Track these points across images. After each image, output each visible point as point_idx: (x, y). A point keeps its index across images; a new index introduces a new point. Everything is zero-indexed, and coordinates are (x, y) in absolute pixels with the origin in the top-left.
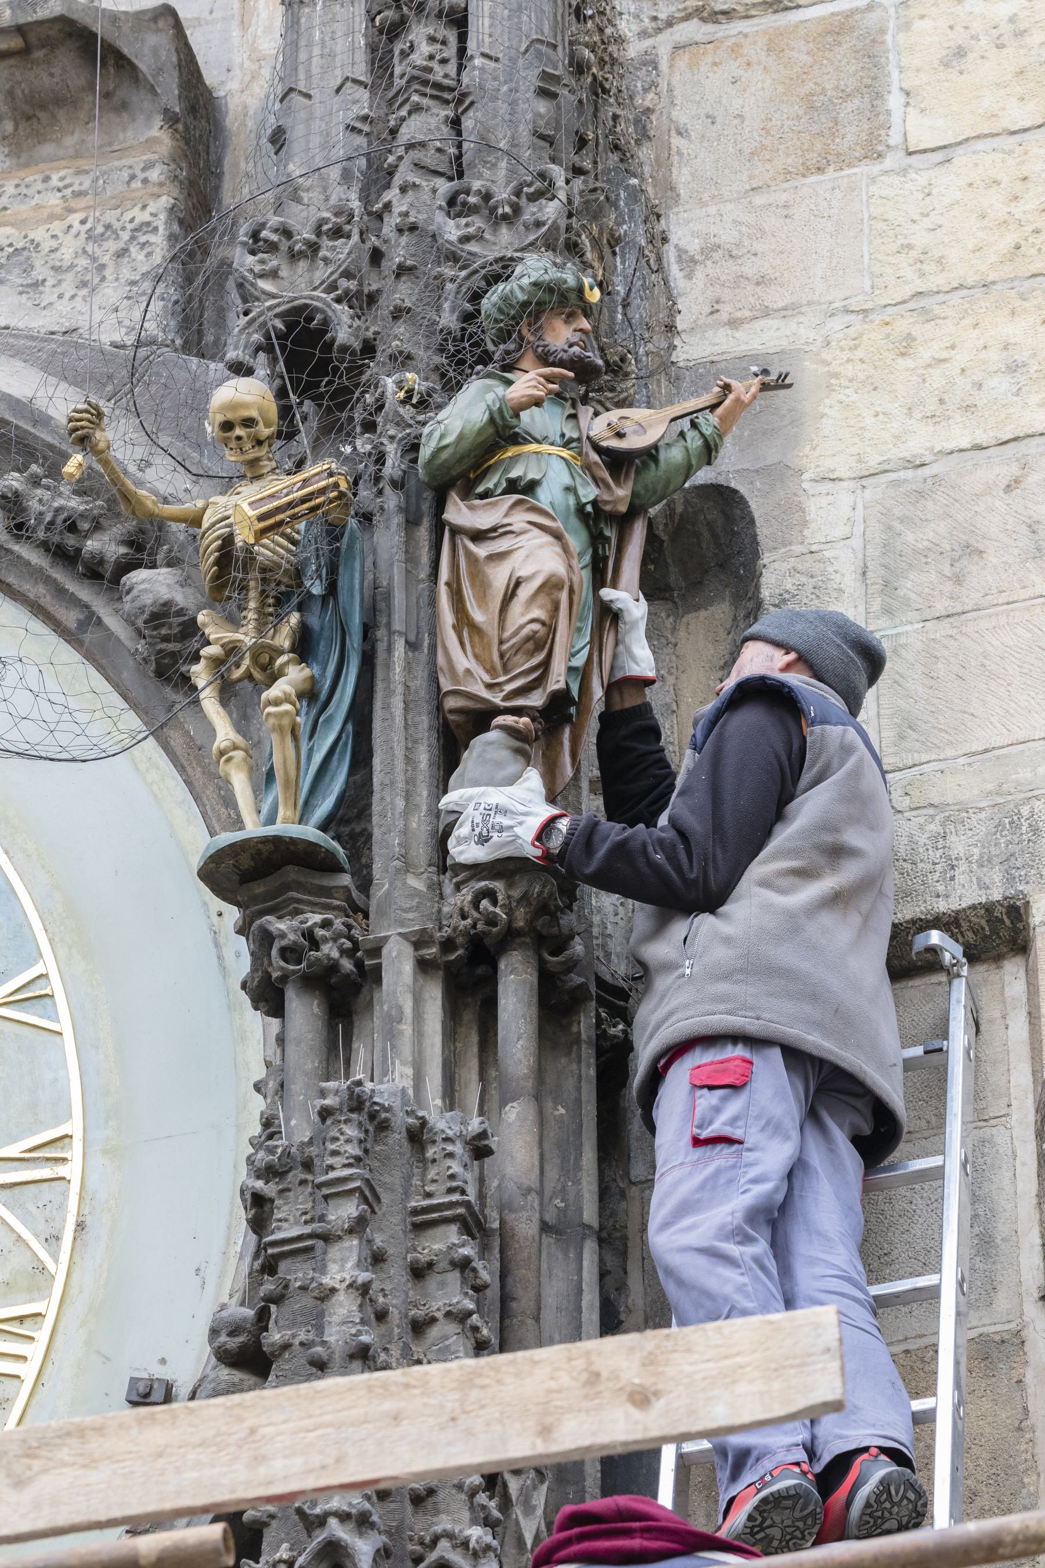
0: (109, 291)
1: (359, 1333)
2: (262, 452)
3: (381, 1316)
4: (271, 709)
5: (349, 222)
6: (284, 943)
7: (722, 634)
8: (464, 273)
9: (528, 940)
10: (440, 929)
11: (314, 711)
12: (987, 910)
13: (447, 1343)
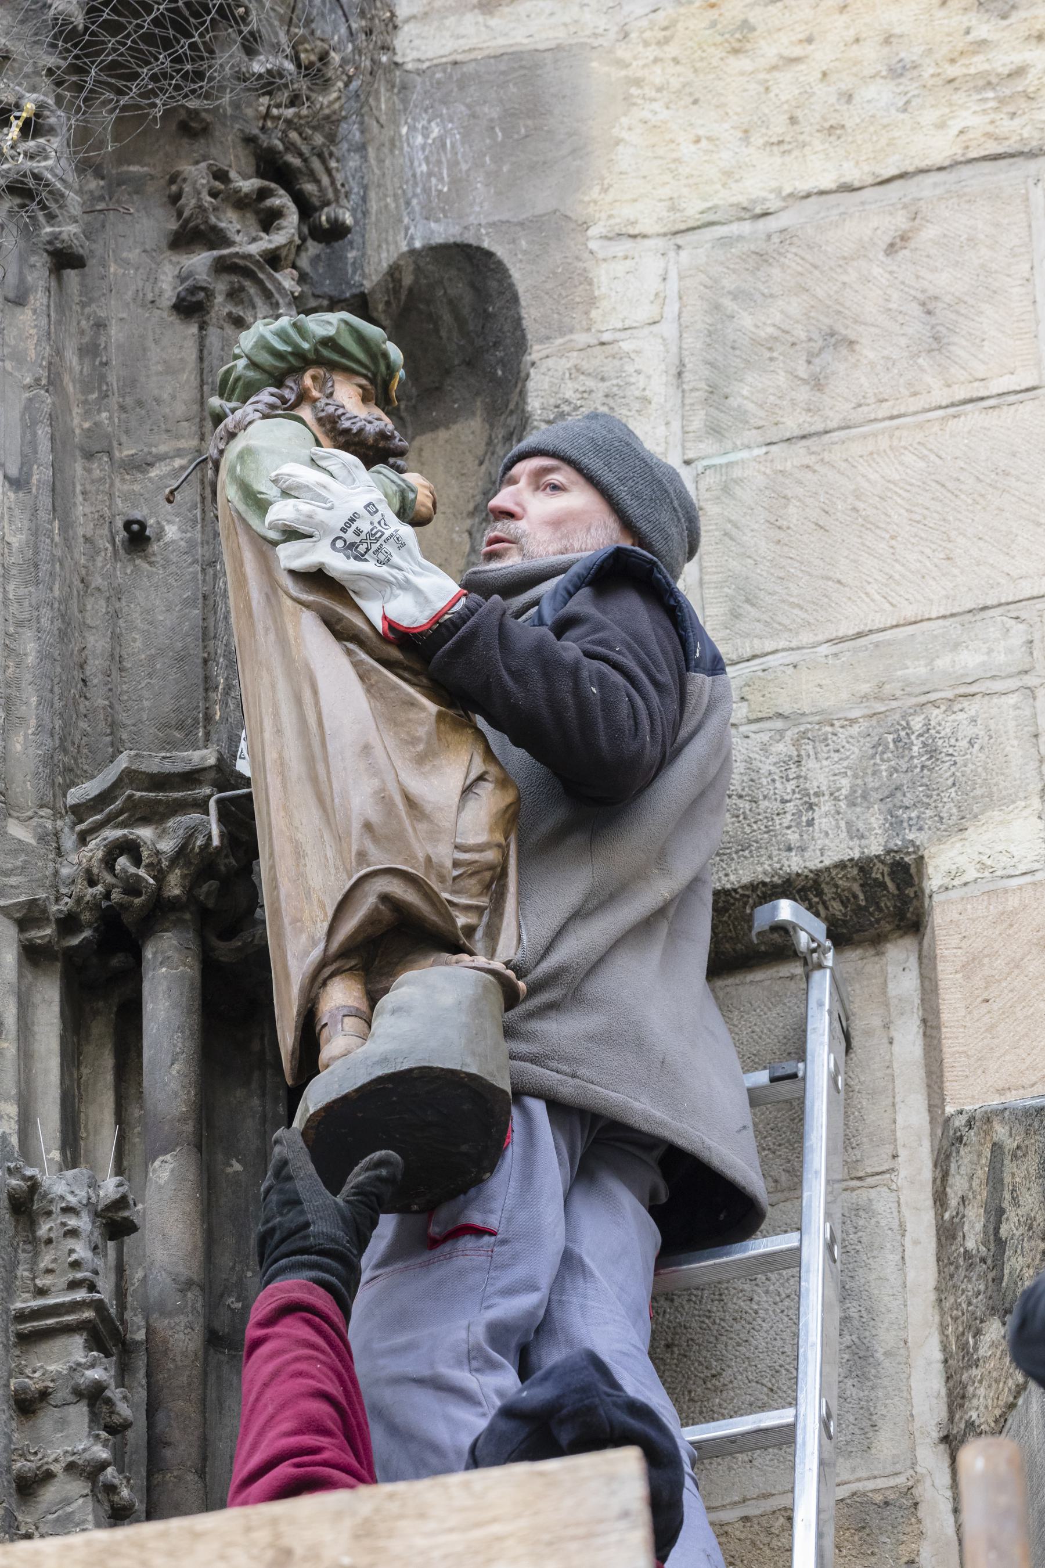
7: (471, 463)
9: (187, 916)
10: (57, 900)
12: (862, 869)
13: (69, 1509)
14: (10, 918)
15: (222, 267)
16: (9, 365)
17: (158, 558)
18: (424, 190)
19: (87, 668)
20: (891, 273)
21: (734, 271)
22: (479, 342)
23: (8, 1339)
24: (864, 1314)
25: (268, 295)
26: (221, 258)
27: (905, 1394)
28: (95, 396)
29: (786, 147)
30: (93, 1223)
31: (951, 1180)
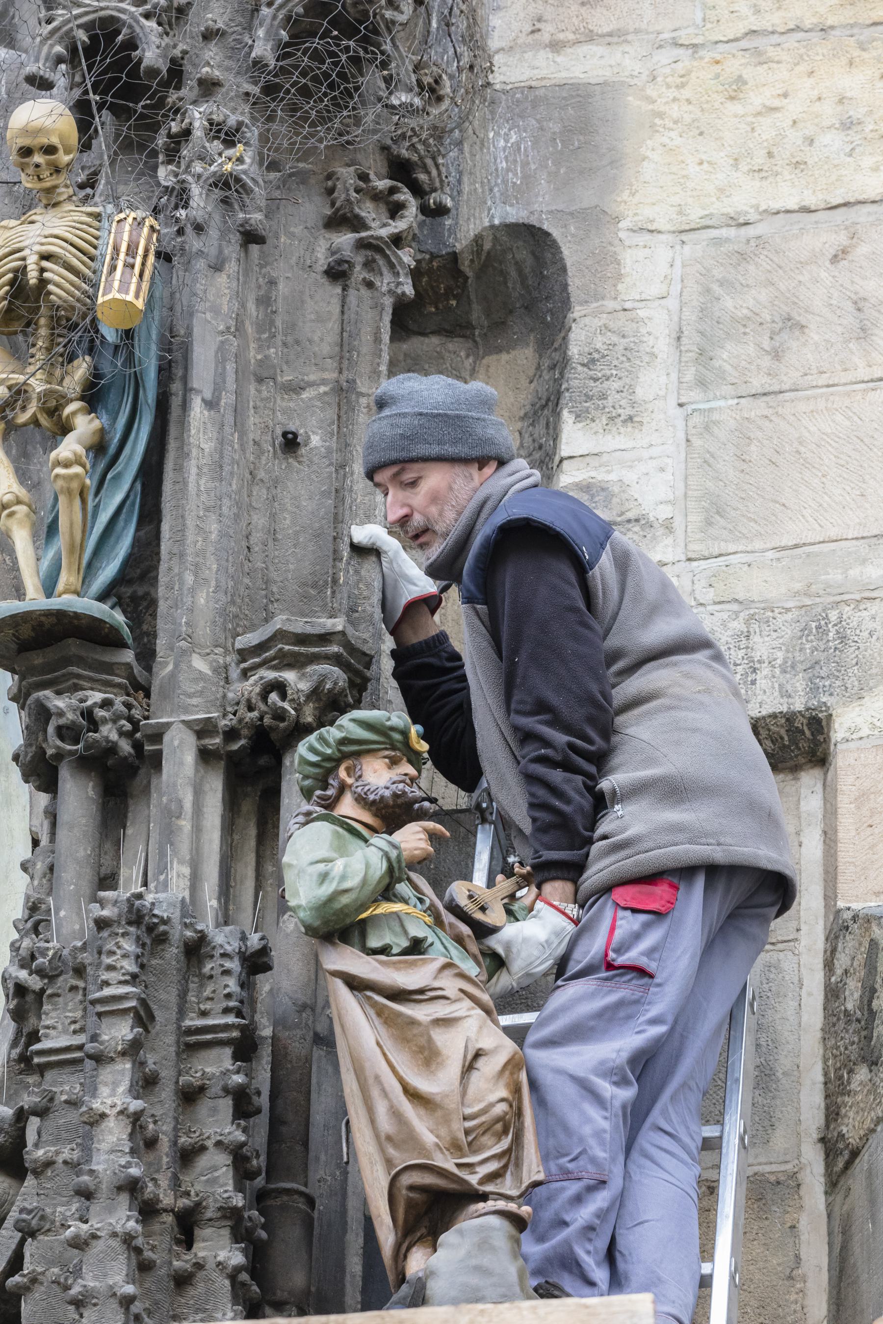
1: (128, 1165)
2: (61, 179)
3: (151, 1143)
4: (59, 470)
6: (62, 721)
7: (524, 382)
10: (224, 715)
11: (102, 466)
12: (788, 720)
13: (216, 1174)
15: (361, 245)
16: (208, 316)
17: (305, 459)
18: (503, 181)
19: (251, 538)
20: (834, 277)
21: (722, 265)
22: (535, 294)
23: (179, 1047)
24: (770, 1043)
25: (392, 266)
26: (361, 239)
27: (796, 1105)
28: (266, 335)
29: (764, 174)
31: (838, 955)
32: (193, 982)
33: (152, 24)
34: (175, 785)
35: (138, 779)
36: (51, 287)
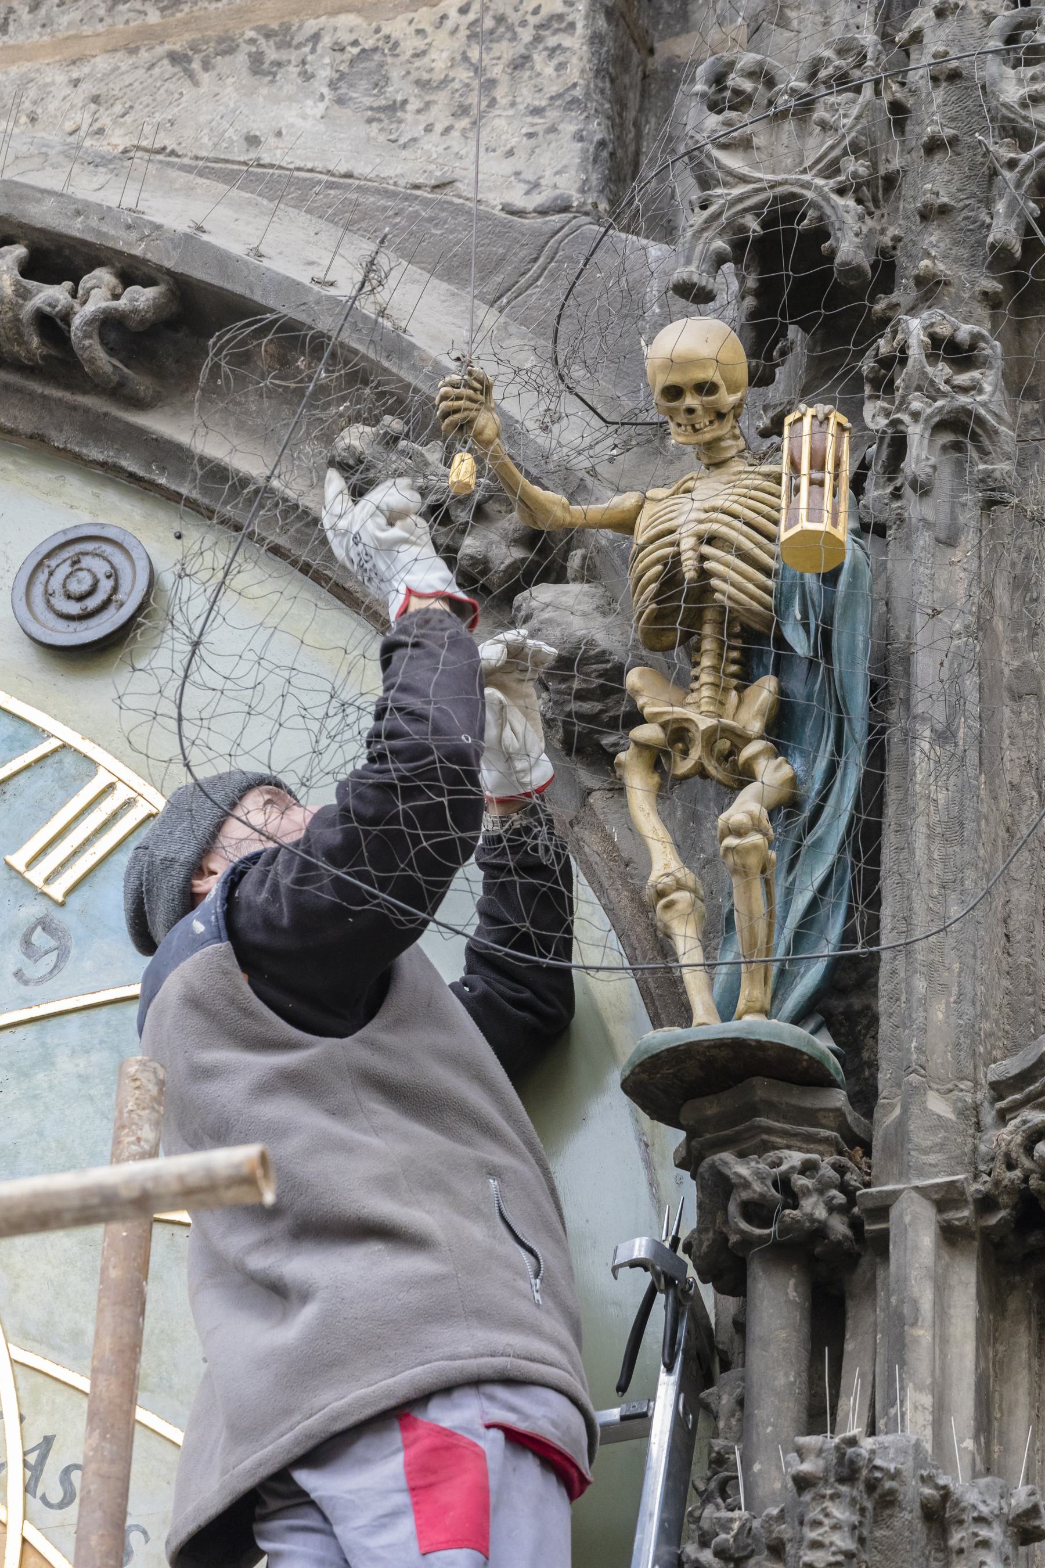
0: (500, 123)
2: (724, 429)
4: (731, 841)
5: (859, 66)
6: (745, 1195)
8: (1025, 157)
10: (976, 1177)
14: (929, 1199)
30: (1005, 1532)
32: (936, 1559)
33: (850, 202)
34: (906, 1279)
35: (859, 1271)
36: (715, 582)
